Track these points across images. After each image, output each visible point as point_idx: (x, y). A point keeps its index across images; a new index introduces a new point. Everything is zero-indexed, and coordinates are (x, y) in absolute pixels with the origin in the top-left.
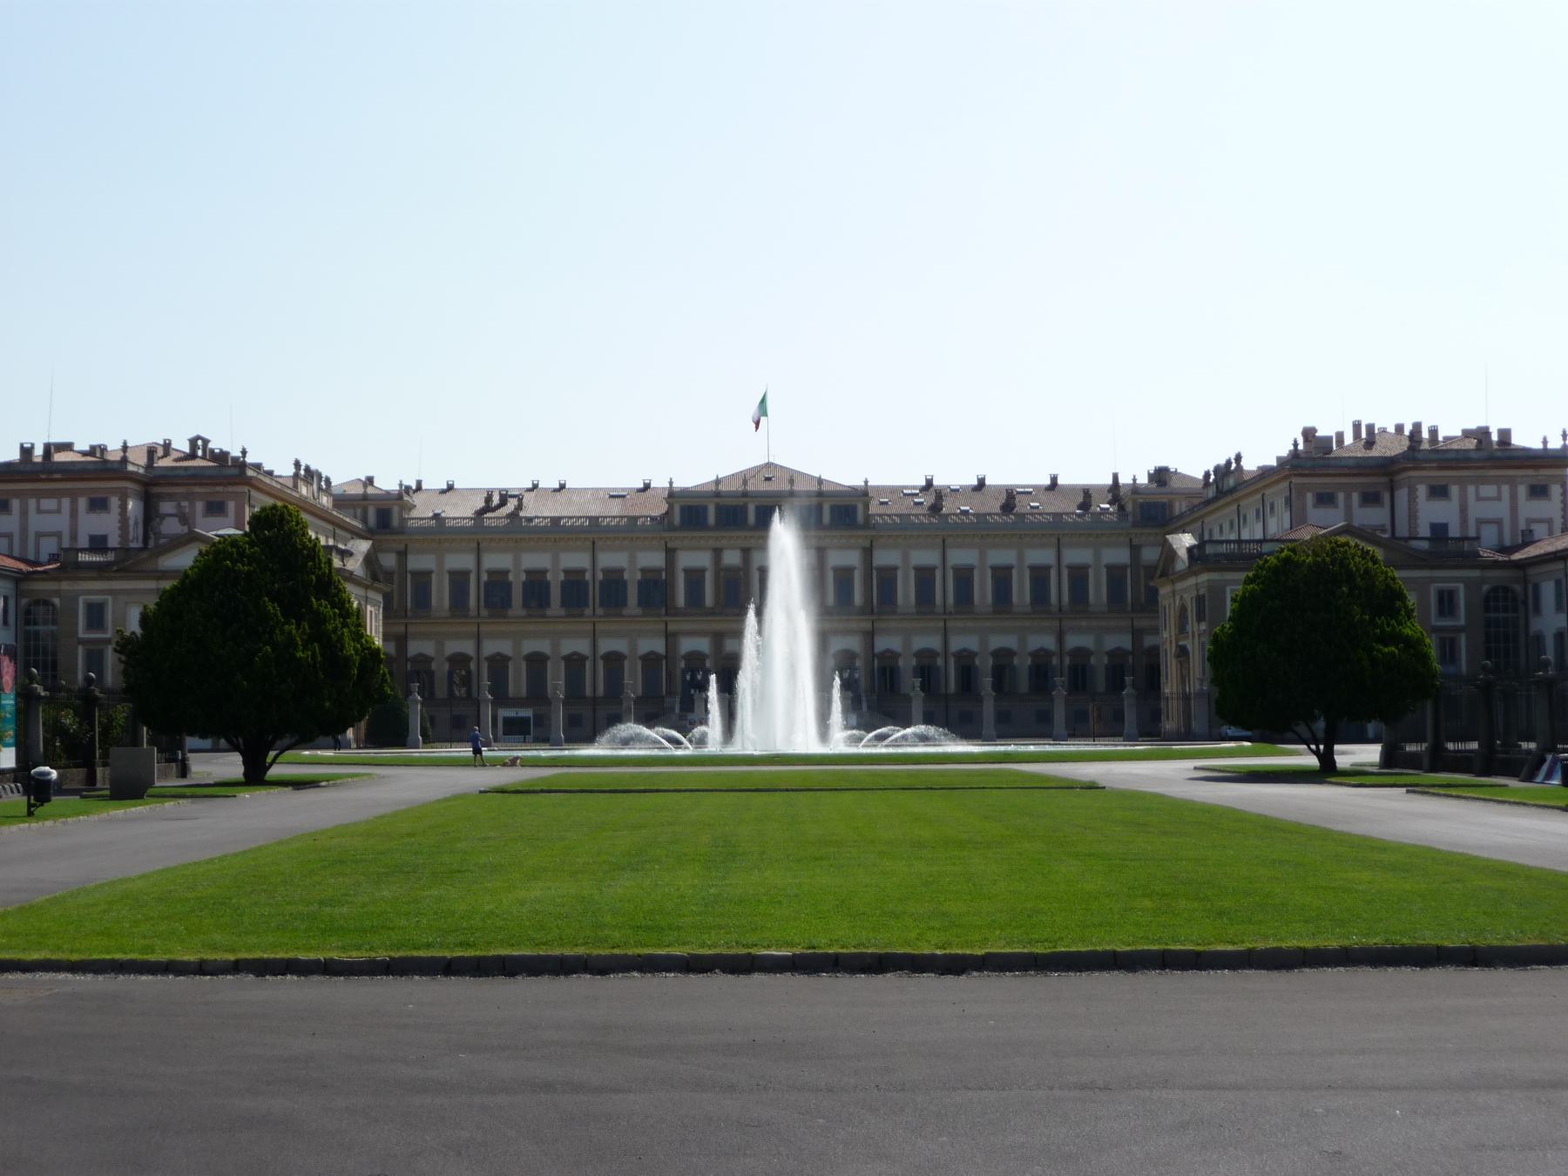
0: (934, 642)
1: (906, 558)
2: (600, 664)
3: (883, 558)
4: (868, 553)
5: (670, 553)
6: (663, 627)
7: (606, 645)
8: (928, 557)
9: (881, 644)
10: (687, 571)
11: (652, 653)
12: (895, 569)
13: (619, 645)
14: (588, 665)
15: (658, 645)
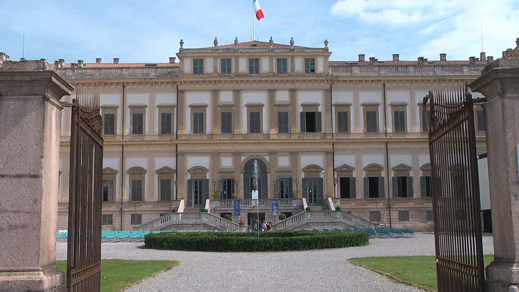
0: (379, 159)
1: (356, 97)
2: (127, 178)
3: (340, 97)
4: (328, 93)
5: (180, 93)
6: (174, 148)
7: (131, 163)
8: (373, 96)
9: (340, 160)
10: (192, 107)
11: (166, 168)
12: (349, 105)
13: (142, 162)
14: (118, 177)
15: (170, 162)
